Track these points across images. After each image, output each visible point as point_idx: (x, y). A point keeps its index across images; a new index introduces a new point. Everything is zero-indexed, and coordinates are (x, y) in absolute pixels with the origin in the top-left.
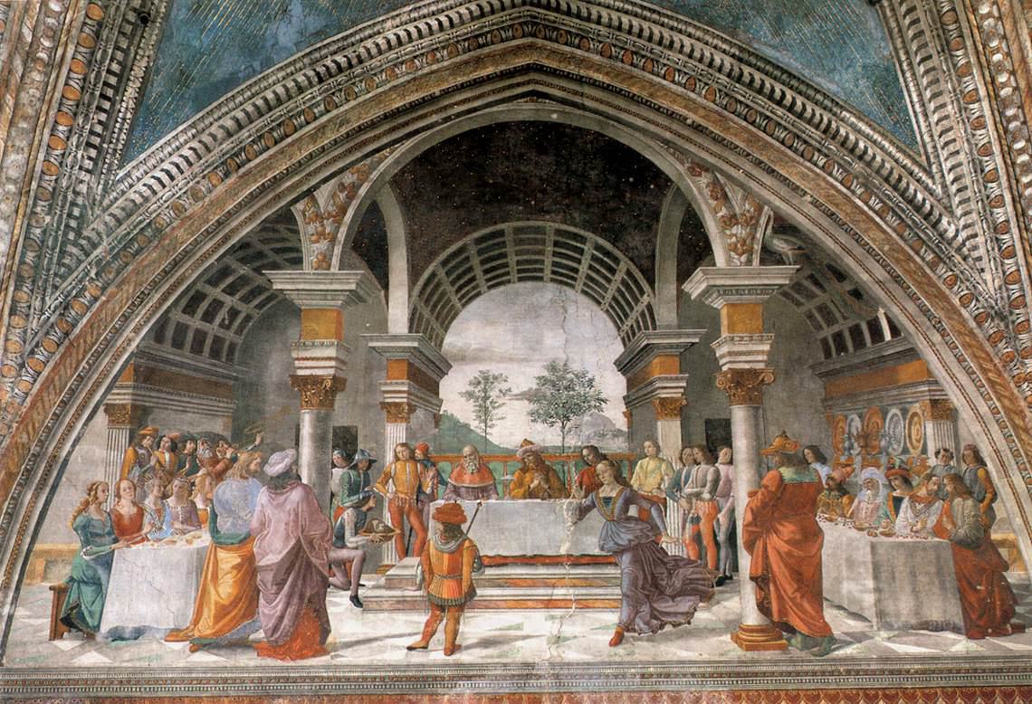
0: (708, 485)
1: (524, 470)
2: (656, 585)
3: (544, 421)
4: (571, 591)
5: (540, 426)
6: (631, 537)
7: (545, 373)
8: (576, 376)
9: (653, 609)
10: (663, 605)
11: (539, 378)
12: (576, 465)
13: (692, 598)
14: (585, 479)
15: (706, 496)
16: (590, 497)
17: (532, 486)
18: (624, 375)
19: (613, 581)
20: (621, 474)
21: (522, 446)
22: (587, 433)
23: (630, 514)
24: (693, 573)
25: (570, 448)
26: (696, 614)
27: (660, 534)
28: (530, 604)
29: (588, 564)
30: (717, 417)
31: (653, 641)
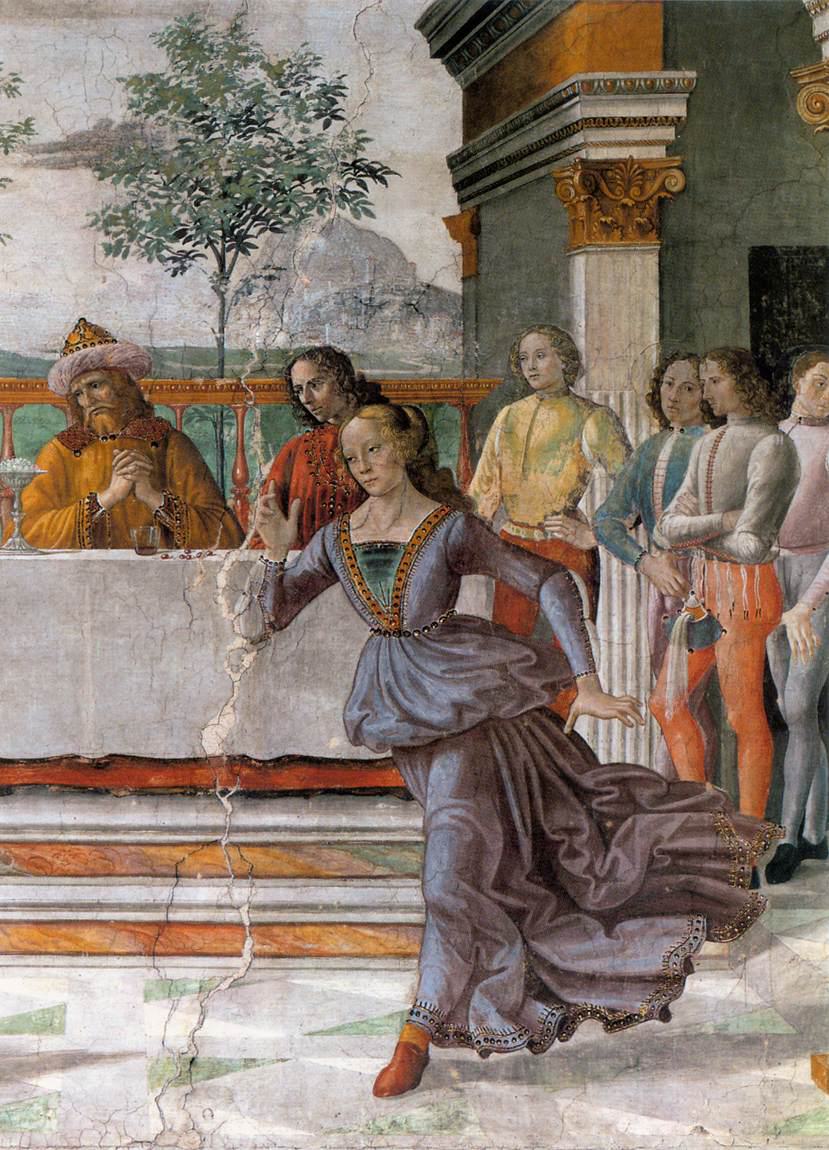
0: (752, 501)
1: (77, 440)
2: (547, 869)
3: (153, 251)
4: (241, 892)
5: (134, 270)
6: (463, 693)
7: (160, 63)
8: (275, 72)
9: (534, 959)
10: (572, 947)
11: (137, 83)
12: (267, 423)
13: (671, 922)
14: (300, 467)
15: (743, 541)
16: (315, 545)
17: (103, 499)
18: (454, 71)
19: (395, 856)
20: (432, 463)
21: (68, 348)
22: (311, 298)
23: (459, 610)
24: (685, 830)
25: (245, 354)
26: (693, 985)
27: (570, 684)
28: (90, 936)
29: (305, 794)
30: (797, 240)
31: (532, 1080)
